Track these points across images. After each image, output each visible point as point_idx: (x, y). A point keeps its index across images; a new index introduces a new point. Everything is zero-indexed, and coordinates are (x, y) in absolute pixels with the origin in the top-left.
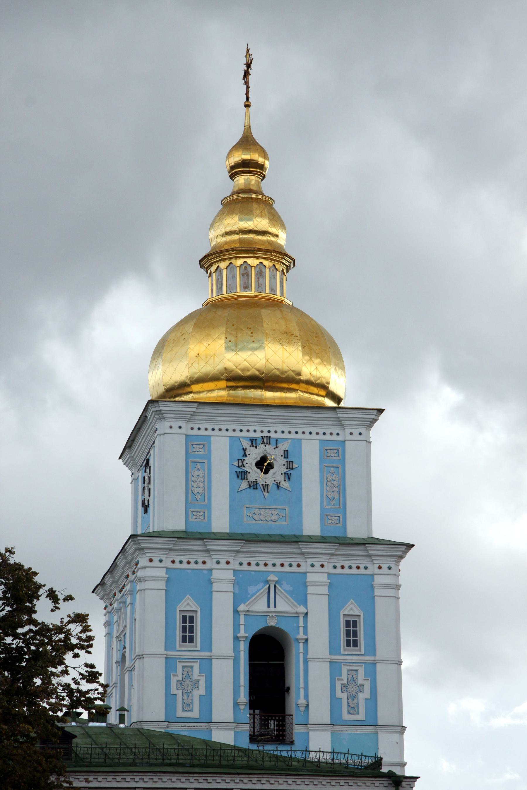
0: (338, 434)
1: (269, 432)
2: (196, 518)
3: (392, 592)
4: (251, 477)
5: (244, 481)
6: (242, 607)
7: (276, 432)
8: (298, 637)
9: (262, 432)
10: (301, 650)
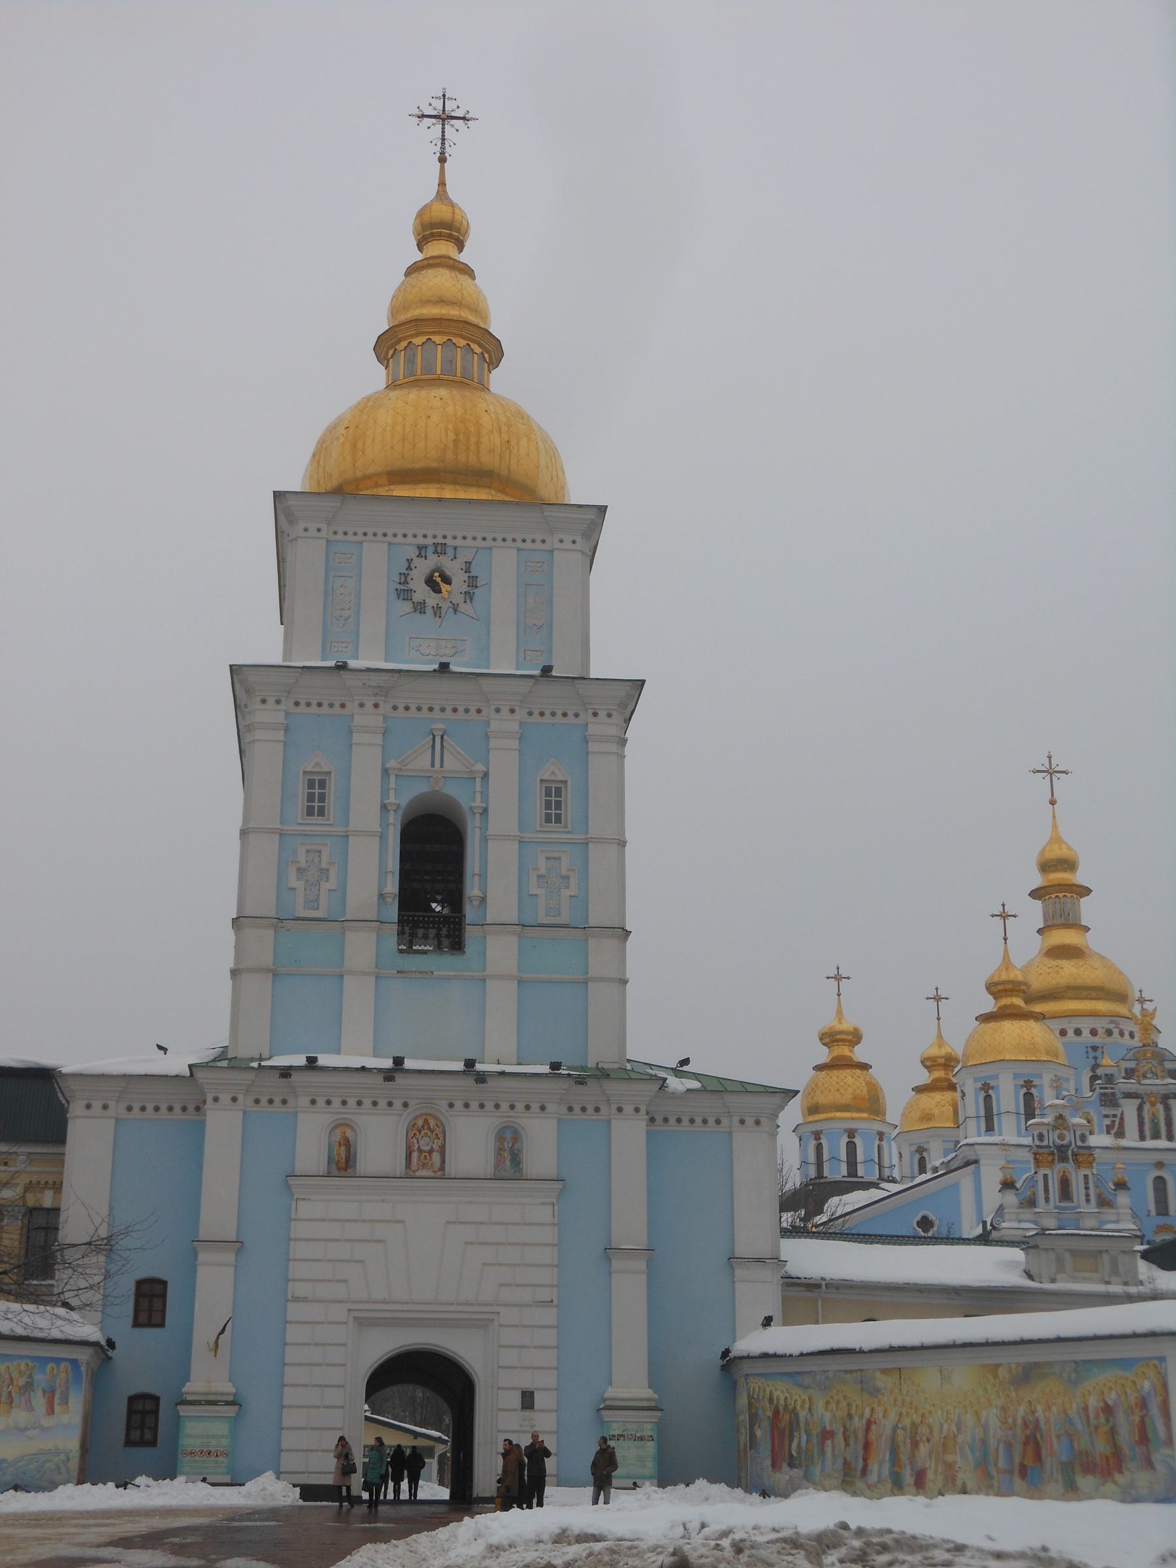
0: (543, 541)
1: (445, 537)
2: (337, 651)
3: (613, 748)
4: (417, 597)
5: (406, 603)
6: (392, 764)
7: (455, 538)
8: (473, 805)
9: (435, 537)
10: (477, 823)
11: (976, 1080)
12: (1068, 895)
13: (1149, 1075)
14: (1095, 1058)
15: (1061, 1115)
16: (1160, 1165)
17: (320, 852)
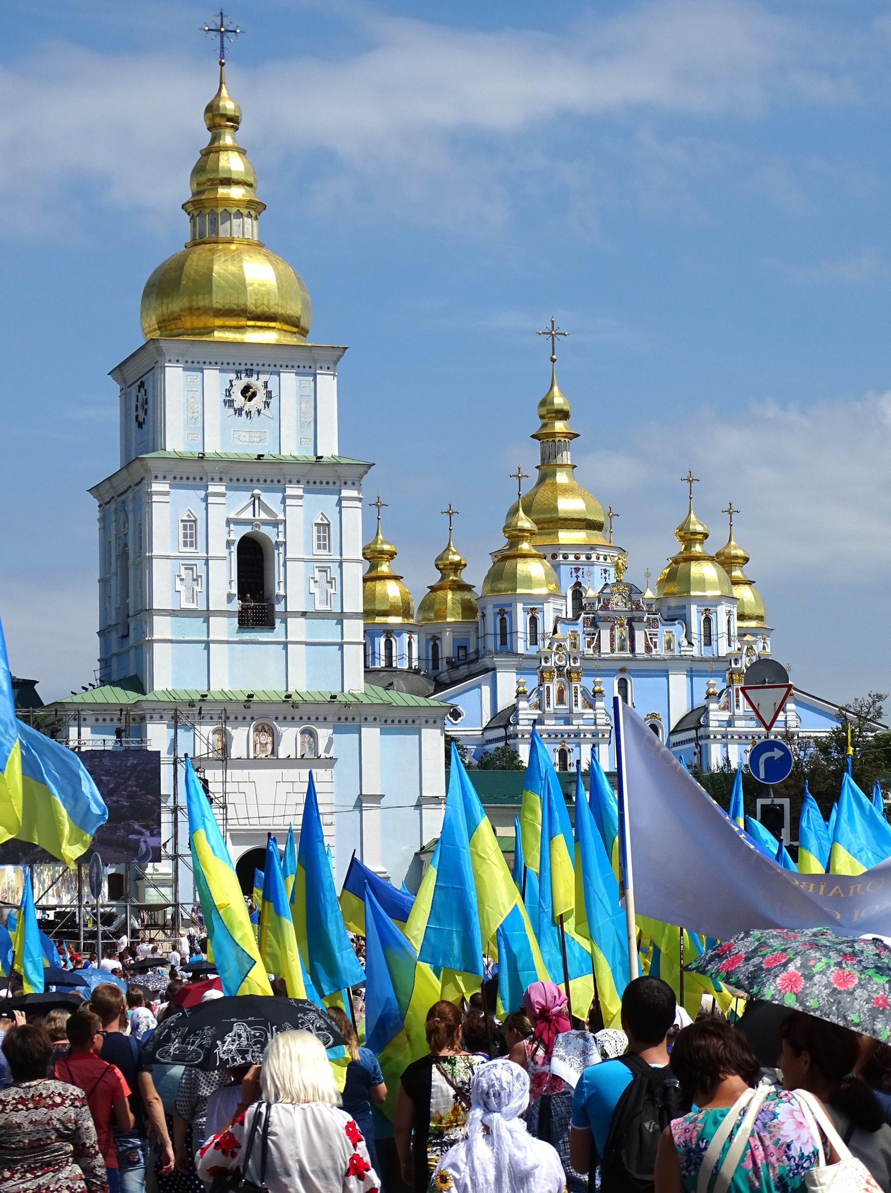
0: (310, 367)
4: (237, 405)
6: (232, 515)
9: (246, 364)
11: (495, 606)
12: (563, 440)
13: (620, 604)
14: (577, 577)
15: (561, 645)
16: (623, 670)
17: (192, 569)
